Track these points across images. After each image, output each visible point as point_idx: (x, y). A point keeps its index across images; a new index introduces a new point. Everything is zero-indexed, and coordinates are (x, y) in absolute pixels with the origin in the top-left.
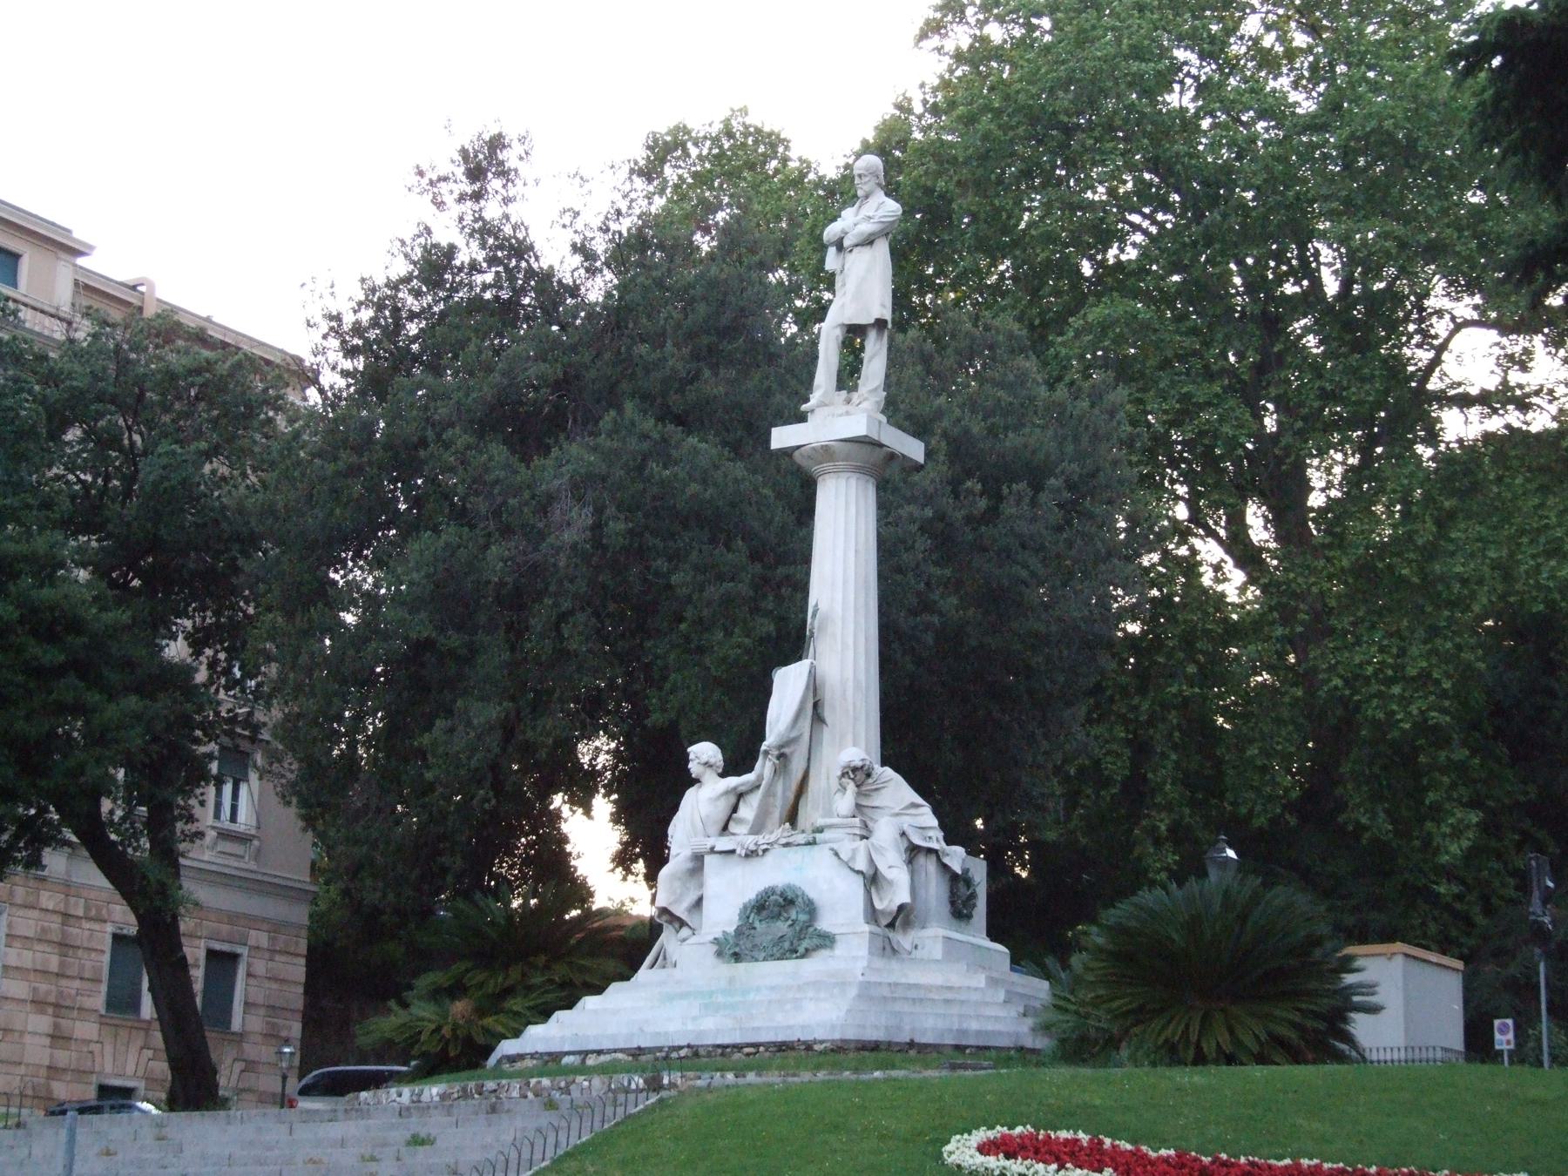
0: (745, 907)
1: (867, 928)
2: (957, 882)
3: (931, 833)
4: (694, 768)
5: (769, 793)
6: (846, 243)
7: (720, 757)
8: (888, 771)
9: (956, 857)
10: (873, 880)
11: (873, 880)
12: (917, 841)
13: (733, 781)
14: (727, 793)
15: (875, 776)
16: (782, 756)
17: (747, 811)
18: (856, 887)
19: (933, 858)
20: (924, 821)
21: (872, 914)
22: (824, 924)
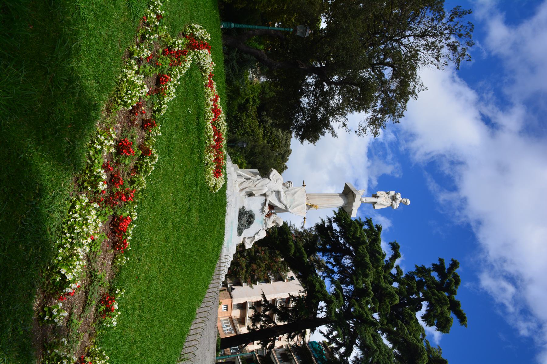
6: (394, 202)
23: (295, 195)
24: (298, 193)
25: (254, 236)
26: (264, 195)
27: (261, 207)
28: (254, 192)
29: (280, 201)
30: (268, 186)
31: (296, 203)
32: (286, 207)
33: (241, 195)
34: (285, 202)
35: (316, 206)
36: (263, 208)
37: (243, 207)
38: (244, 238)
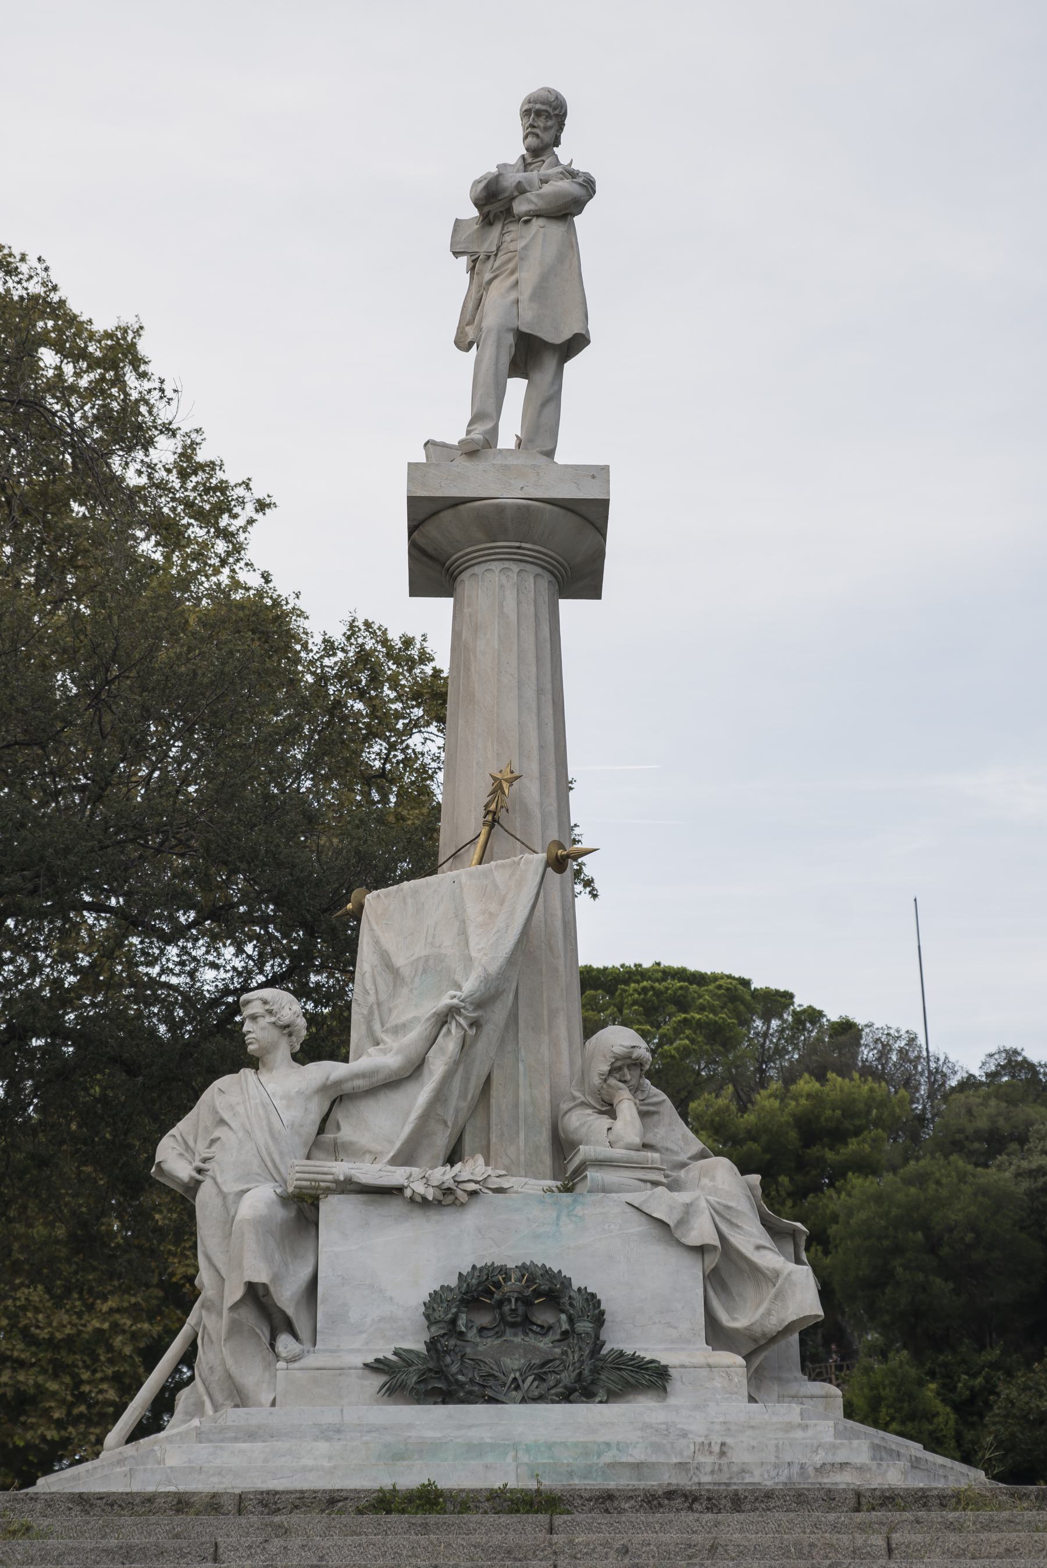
4: (256, 1033)
5: (439, 1097)
6: (520, 207)
14: (324, 1089)
16: (475, 1024)
23: (400, 961)
24: (389, 941)
25: (701, 1250)
26: (303, 1209)
28: (238, 1293)
29: (416, 1069)
30: (231, 1187)
31: (447, 942)
32: (444, 1018)
33: (266, 1398)
34: (414, 1036)
35: (497, 789)
36: (423, 1204)
37: (378, 1367)
38: (717, 1334)
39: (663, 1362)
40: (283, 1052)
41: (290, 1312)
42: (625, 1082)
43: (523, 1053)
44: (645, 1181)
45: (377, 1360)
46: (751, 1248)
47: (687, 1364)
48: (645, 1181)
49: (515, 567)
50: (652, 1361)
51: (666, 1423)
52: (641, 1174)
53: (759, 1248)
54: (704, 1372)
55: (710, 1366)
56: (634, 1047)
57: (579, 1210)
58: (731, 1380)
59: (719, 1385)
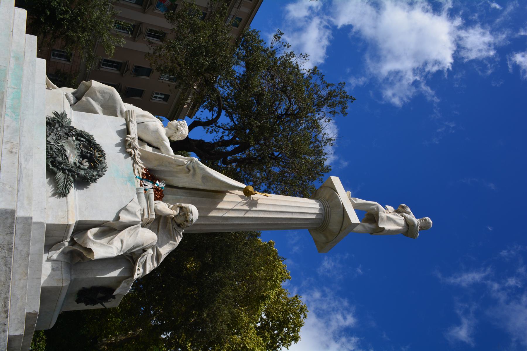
0: (91, 136)
1: (72, 222)
2: (106, 291)
3: (141, 270)
7: (180, 139)
8: (179, 239)
9: (124, 290)
10: (109, 229)
11: (109, 229)
12: (140, 261)
13: (168, 143)
15: (178, 229)
17: (149, 149)
18: (107, 216)
19: (127, 275)
20: (148, 265)
21: (82, 227)
22: (74, 192)
27: (118, 139)
39: (68, 196)
40: (171, 132)
41: (84, 99)
42: (179, 213)
43: (184, 198)
44: (143, 211)
45: (66, 115)
46: (122, 238)
47: (68, 203)
48: (143, 211)
49: (322, 208)
50: (69, 192)
51: (32, 155)
52: (146, 210)
53: (122, 241)
54: (65, 209)
55: (68, 211)
56: (192, 213)
57: (129, 184)
58: (62, 218)
59: (59, 214)
